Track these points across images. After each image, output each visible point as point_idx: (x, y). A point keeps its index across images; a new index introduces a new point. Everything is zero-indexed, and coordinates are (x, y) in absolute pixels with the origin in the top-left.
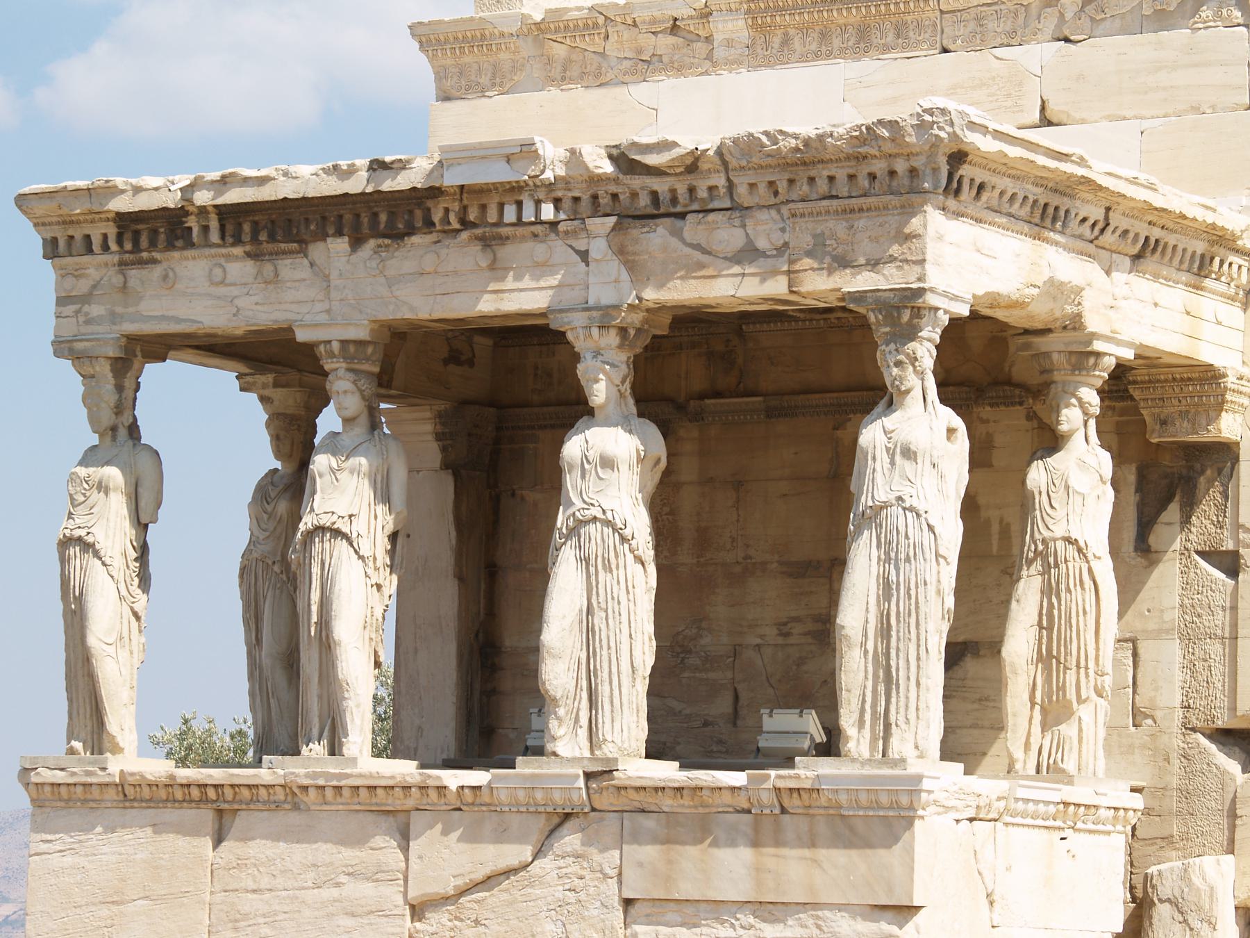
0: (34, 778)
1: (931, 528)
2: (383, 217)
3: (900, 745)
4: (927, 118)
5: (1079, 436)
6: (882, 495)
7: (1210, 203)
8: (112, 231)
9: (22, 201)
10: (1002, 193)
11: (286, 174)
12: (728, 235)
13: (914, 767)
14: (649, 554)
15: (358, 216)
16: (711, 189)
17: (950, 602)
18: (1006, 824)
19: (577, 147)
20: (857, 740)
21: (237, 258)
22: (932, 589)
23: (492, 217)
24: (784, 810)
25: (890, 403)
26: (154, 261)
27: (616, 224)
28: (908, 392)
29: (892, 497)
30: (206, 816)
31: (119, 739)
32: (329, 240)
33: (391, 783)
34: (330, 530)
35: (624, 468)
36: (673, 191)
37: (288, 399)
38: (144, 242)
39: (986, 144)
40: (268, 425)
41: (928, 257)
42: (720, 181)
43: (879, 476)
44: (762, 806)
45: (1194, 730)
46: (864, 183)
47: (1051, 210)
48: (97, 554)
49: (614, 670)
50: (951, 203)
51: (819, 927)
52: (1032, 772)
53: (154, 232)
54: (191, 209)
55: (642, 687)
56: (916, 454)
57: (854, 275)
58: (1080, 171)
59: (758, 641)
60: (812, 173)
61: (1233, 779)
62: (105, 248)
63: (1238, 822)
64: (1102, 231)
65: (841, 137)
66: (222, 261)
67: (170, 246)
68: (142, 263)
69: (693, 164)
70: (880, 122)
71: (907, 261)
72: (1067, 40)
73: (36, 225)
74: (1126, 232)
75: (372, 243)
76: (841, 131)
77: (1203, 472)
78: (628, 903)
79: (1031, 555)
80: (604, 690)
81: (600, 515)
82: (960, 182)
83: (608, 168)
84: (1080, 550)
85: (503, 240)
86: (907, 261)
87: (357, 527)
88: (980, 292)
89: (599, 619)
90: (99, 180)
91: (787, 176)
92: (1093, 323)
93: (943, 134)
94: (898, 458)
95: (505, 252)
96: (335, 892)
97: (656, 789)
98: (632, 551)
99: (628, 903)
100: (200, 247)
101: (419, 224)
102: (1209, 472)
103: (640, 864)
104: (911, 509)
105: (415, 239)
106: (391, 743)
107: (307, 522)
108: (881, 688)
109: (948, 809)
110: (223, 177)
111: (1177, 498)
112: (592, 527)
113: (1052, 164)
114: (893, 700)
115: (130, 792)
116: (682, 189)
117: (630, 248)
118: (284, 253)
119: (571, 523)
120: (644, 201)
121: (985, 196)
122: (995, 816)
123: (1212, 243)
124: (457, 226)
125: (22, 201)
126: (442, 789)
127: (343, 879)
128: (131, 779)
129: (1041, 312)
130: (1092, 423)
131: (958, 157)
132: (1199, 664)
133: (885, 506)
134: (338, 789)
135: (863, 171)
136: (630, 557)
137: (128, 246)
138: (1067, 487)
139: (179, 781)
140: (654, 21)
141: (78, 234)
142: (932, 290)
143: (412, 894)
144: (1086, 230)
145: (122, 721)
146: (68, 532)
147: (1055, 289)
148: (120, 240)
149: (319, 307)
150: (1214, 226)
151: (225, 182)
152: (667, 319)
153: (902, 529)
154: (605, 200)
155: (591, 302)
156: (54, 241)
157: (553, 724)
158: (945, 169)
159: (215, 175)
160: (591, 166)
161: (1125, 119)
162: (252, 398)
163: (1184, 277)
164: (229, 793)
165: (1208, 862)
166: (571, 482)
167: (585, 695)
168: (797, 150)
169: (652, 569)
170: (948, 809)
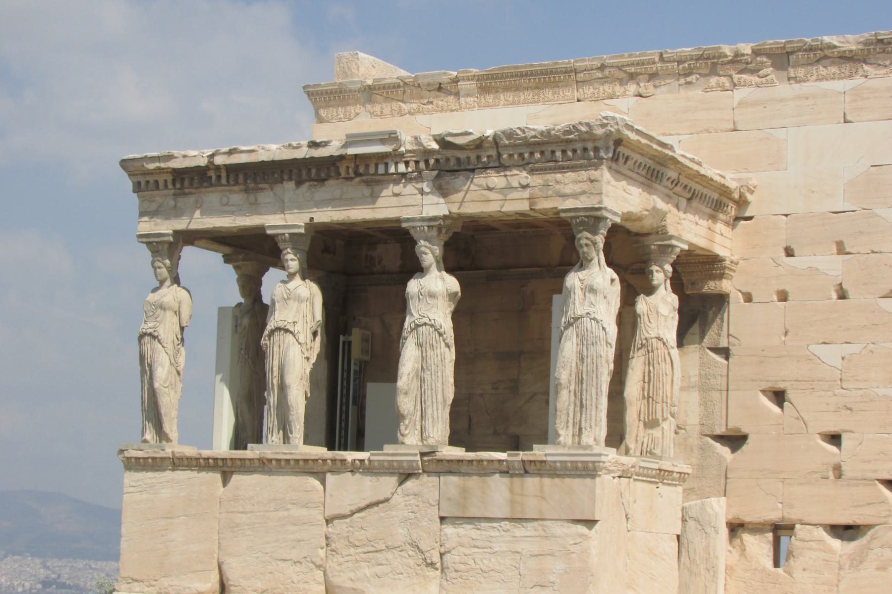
0: (127, 454)
1: (604, 329)
2: (314, 171)
3: (587, 438)
4: (605, 121)
5: (663, 287)
6: (580, 311)
7: (722, 173)
8: (170, 178)
9: (125, 164)
10: (636, 162)
11: (263, 149)
12: (496, 179)
13: (596, 450)
14: (451, 341)
16: (489, 157)
17: (612, 366)
18: (635, 480)
19: (418, 135)
20: (565, 435)
21: (235, 192)
22: (603, 359)
23: (372, 170)
24: (526, 472)
25: (581, 266)
26: (191, 194)
27: (438, 176)
28: (591, 260)
29: (584, 312)
31: (170, 435)
33: (316, 458)
34: (283, 329)
35: (440, 298)
36: (468, 158)
37: (250, 267)
38: (186, 183)
39: (633, 136)
40: (238, 280)
41: (604, 192)
42: (493, 153)
43: (577, 302)
44: (514, 469)
45: (707, 435)
46: (570, 154)
47: (656, 172)
48: (159, 341)
49: (434, 401)
50: (614, 165)
51: (544, 531)
52: (638, 454)
53: (192, 179)
54: (211, 167)
55: (448, 410)
56: (593, 291)
57: (564, 201)
58: (671, 153)
59: (482, 392)
60: (543, 149)
61: (725, 460)
62: (166, 186)
63: (728, 481)
64: (676, 185)
65: (559, 131)
66: (227, 193)
67: (201, 186)
68: (185, 194)
69: (479, 144)
70: (580, 123)
71: (591, 193)
72: (641, 96)
73: (129, 175)
74: (686, 186)
75: (307, 184)
76: (559, 127)
77: (711, 309)
78: (442, 519)
79: (640, 346)
80: (429, 411)
81: (428, 322)
82: (618, 155)
83: (435, 146)
84: (664, 344)
85: (379, 182)
86: (591, 193)
87: (298, 328)
88: (625, 211)
89: (427, 376)
90: (165, 152)
91: (529, 150)
92: (671, 231)
93: (613, 130)
94: (587, 294)
96: (286, 513)
98: (444, 340)
99: (442, 519)
100: (216, 186)
101: (333, 174)
103: (450, 499)
104: (594, 319)
106: (308, 441)
107: (271, 325)
108: (578, 409)
109: (613, 471)
110: (230, 150)
113: (659, 149)
114: (584, 416)
115: (176, 461)
117: (445, 187)
119: (413, 325)
121: (629, 163)
122: (629, 475)
123: (721, 194)
124: (353, 175)
125: (125, 164)
126: (343, 461)
127: (290, 506)
128: (177, 455)
129: (648, 223)
130: (668, 281)
131: (618, 142)
132: (709, 403)
133: (581, 317)
134: (288, 461)
135: (571, 147)
136: (443, 344)
137: (178, 186)
138: (657, 312)
140: (429, 85)
142: (605, 209)
143: (327, 514)
144: (669, 184)
145: (171, 427)
146: (144, 331)
147: (655, 210)
150: (724, 185)
151: (231, 152)
152: (460, 224)
153: (589, 329)
154: (432, 162)
155: (424, 215)
156: (139, 183)
157: (402, 428)
158: (612, 148)
159: (226, 149)
160: (425, 144)
161: (670, 135)
162: (230, 267)
163: (708, 211)
164: (229, 463)
165: (713, 500)
166: (413, 305)
167: (419, 413)
168: (535, 137)
169: (453, 349)
170: (613, 471)
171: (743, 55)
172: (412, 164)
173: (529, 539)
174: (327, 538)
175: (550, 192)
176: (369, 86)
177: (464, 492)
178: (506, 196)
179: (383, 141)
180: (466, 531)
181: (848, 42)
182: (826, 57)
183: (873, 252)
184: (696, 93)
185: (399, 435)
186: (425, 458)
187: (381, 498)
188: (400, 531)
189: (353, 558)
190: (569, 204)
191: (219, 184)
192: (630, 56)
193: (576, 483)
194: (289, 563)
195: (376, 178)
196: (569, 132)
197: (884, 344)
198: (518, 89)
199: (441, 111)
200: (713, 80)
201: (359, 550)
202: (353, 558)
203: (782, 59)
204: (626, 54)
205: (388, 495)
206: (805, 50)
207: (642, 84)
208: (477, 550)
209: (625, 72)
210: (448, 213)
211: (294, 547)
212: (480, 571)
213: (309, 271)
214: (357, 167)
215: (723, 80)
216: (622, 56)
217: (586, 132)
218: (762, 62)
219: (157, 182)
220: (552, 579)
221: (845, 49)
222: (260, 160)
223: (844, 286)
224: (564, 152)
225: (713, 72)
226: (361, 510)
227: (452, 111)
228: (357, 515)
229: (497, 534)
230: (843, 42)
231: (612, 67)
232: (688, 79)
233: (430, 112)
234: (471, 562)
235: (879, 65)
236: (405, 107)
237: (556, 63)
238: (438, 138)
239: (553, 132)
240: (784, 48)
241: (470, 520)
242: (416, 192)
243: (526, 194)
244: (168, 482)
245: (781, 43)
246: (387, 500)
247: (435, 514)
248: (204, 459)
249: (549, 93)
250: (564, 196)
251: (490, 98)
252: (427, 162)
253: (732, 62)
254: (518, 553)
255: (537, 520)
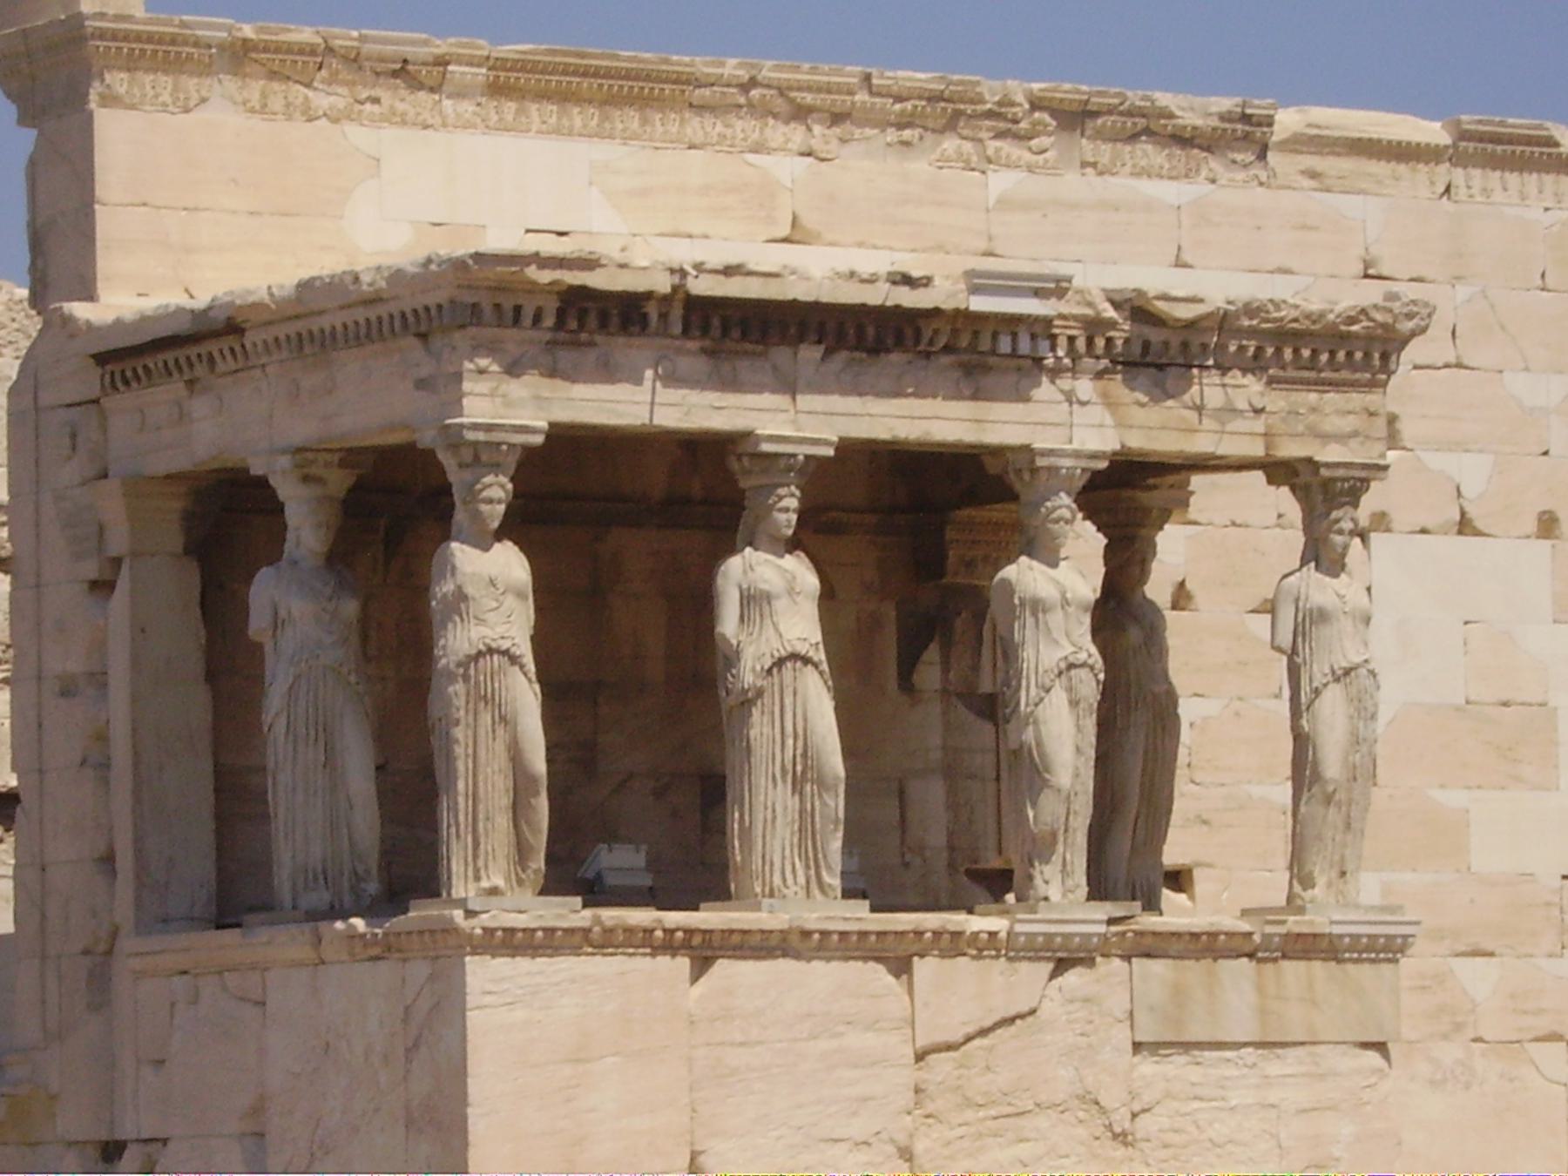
2: (871, 331)
8: (551, 305)
15: (841, 325)
21: (689, 352)
23: (985, 344)
30: (683, 963)
32: (802, 346)
36: (1166, 344)
38: (592, 321)
51: (1317, 1064)
57: (1324, 445)
62: (537, 318)
68: (578, 344)
71: (1367, 437)
83: (1110, 313)
85: (987, 369)
86: (1367, 437)
95: (989, 381)
97: (1173, 934)
99: (1137, 1047)
100: (657, 334)
101: (910, 343)
102: (964, 615)
103: (1152, 1009)
105: (895, 357)
111: (937, 638)
112: (1084, 673)
116: (1175, 342)
118: (746, 353)
120: (1137, 349)
126: (957, 935)
127: (841, 1028)
134: (843, 935)
137: (573, 325)
139: (667, 926)
140: (382, 60)
141: (508, 304)
143: (919, 1044)
148: (561, 314)
149: (782, 416)
151: (729, 271)
154: (1100, 343)
155: (1075, 446)
161: (875, 247)
164: (716, 939)
168: (1295, 320)
171: (1013, 104)
172: (1062, 342)
173: (1288, 1080)
174: (917, 1091)
175: (1300, 428)
176: (245, 41)
177: (1178, 993)
178: (1223, 424)
179: (1037, 293)
180: (1176, 1066)
181: (1192, 109)
182: (1147, 131)
183: (1234, 524)
184: (920, 167)
185: (1038, 881)
186: (1114, 929)
187: (1025, 1009)
188: (1063, 1072)
189: (972, 1130)
190: (1330, 454)
191: (664, 332)
192: (813, 71)
193: (1363, 973)
194: (844, 1146)
195: (992, 360)
196: (1352, 320)
197: (1259, 702)
198: (565, 97)
199: (404, 123)
200: (950, 144)
201: (981, 1114)
202: (972, 1130)
203: (1074, 118)
204: (806, 66)
205: (1033, 1005)
206: (1121, 114)
207: (817, 129)
208: (1196, 1105)
209: (792, 101)
210: (1118, 447)
211: (855, 1114)
212: (1209, 1145)
213: (810, 536)
214: (955, 332)
215: (968, 147)
216: (797, 69)
217: (1384, 326)
218: (1039, 122)
219: (518, 309)
220: (1337, 1154)
221: (1187, 122)
222: (790, 297)
223: (1188, 585)
224: (1332, 353)
225: (951, 124)
226: (983, 1032)
227: (426, 127)
228: (977, 1042)
229: (1235, 1073)
230: (1183, 109)
231: (768, 86)
232: (907, 134)
233: (375, 121)
234: (1192, 1129)
235: (1234, 162)
236: (322, 100)
237: (666, 61)
238: (1117, 298)
239: (1331, 317)
240: (1087, 102)
241: (1187, 1046)
242: (1062, 398)
243: (1259, 425)
244: (573, 981)
245: (1084, 93)
246: (1033, 1012)
247: (1123, 1036)
248: (665, 930)
249: (630, 119)
250: (1325, 438)
251: (510, 107)
252: (1090, 342)
253: (990, 115)
254: (1273, 1106)
255: (1302, 1044)
